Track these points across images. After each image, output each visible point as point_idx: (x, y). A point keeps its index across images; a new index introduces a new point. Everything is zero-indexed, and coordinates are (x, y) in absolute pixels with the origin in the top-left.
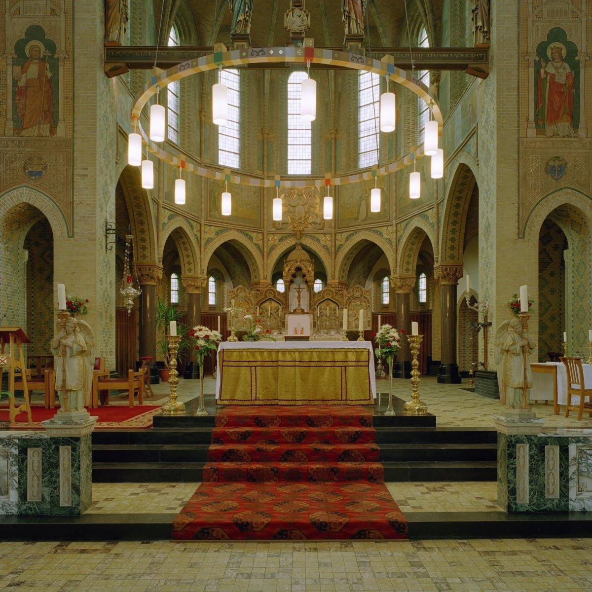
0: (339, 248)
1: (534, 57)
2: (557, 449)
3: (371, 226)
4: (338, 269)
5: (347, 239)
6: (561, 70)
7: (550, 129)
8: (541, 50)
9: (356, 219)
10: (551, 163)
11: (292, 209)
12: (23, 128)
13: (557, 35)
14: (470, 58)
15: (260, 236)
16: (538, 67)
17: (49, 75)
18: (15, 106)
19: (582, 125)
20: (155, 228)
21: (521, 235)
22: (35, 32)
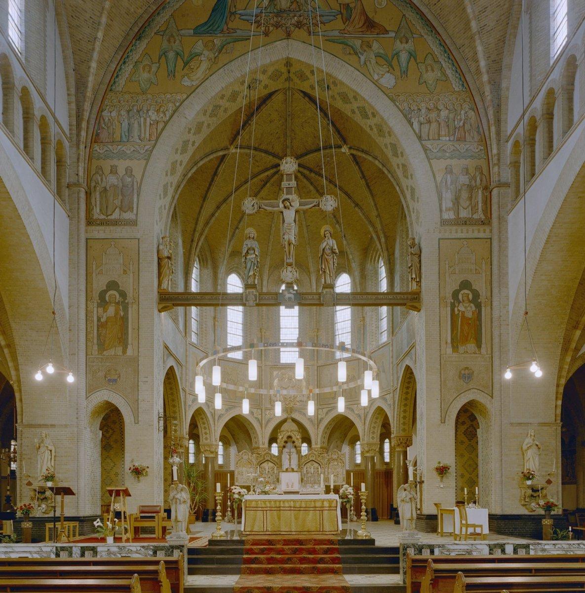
1: (450, 300)
6: (469, 308)
7: (461, 349)
8: (455, 294)
10: (463, 372)
12: (104, 350)
17: (122, 314)
18: (99, 335)
19: (483, 346)
22: (113, 285)
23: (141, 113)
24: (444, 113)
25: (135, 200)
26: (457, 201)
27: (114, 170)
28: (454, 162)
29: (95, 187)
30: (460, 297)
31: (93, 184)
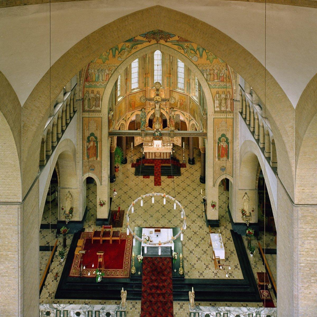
6: (224, 144)
7: (221, 159)
8: (219, 139)
16: (218, 143)
17: (96, 145)
18: (87, 153)
19: (229, 158)
21: (214, 186)
22: (92, 134)
23: (103, 71)
24: (216, 71)
25: (101, 103)
26: (220, 104)
27: (93, 92)
28: (219, 90)
31: (85, 97)
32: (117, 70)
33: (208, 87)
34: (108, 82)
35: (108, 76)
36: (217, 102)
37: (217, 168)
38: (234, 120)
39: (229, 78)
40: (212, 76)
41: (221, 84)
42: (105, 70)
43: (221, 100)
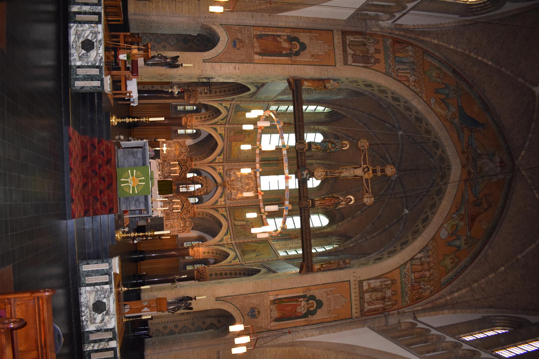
0: (217, 210)
1: (308, 294)
2: (108, 280)
3: (231, 228)
4: (203, 210)
5: (222, 215)
6: (303, 309)
7: (273, 307)
8: (312, 297)
9: (235, 220)
10: (256, 310)
11: (239, 180)
12: (257, 39)
13: (320, 304)
14: (308, 263)
15: (221, 161)
16: (304, 297)
17: (284, 52)
18: (268, 35)
19: (277, 323)
20: (223, 99)
21: (218, 299)
22: (303, 47)
23: (413, 71)
24: (427, 274)
25: (360, 65)
26: (374, 290)
27: (377, 51)
28: (398, 284)
29: (366, 38)
30: (311, 301)
31: (368, 37)
32: (417, 96)
33: (402, 262)
34: (396, 79)
35: (406, 79)
36: (376, 283)
37: (255, 301)
38: (348, 321)
39: (417, 299)
40: (420, 268)
41: (408, 286)
42: (414, 75)
43: (381, 291)
